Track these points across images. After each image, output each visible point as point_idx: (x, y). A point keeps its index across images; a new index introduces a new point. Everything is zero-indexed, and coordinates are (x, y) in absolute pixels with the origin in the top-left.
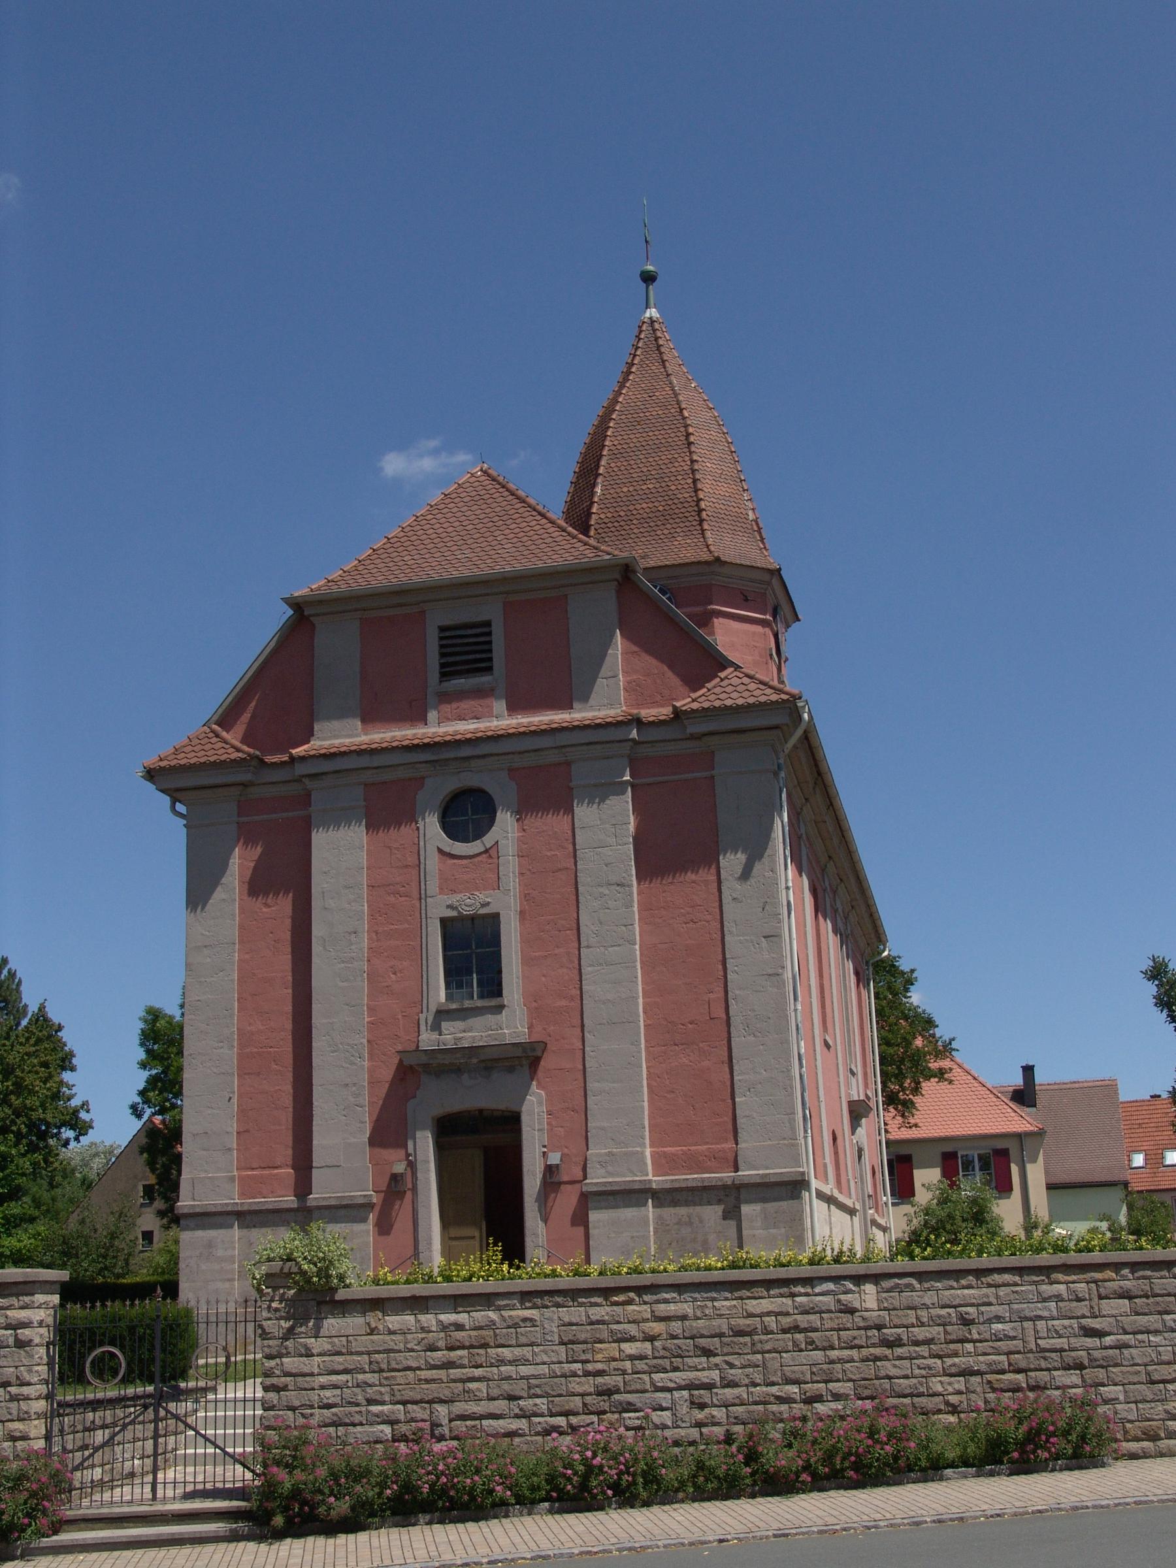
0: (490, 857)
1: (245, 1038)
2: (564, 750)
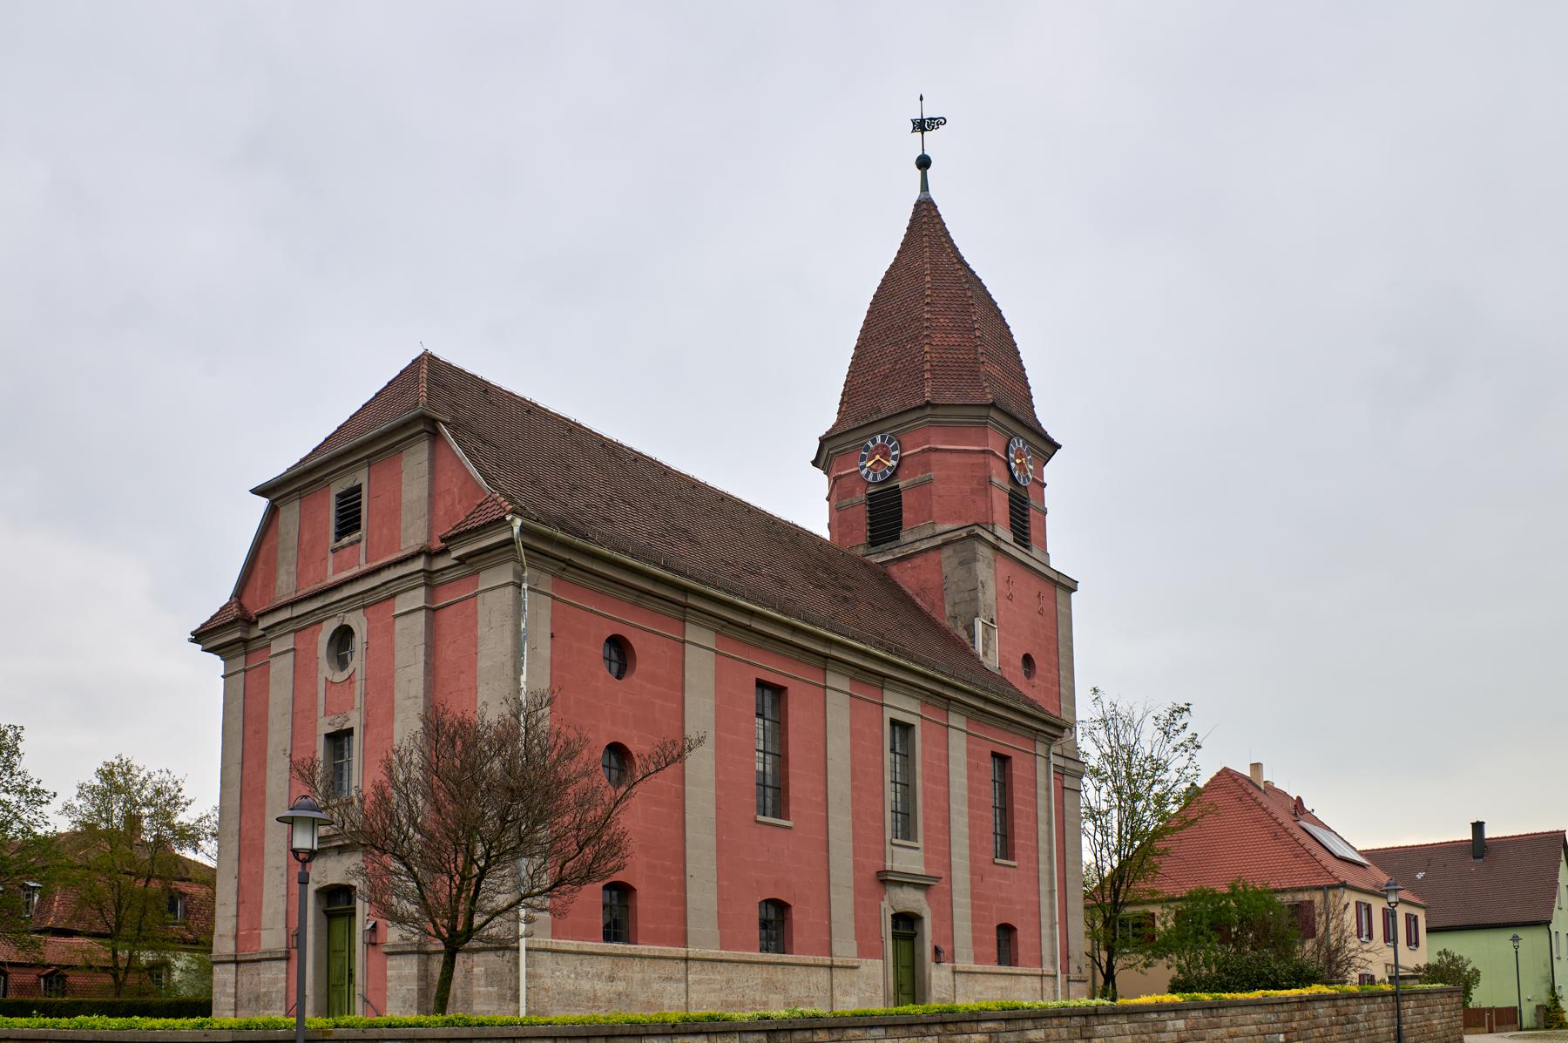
2: (388, 586)
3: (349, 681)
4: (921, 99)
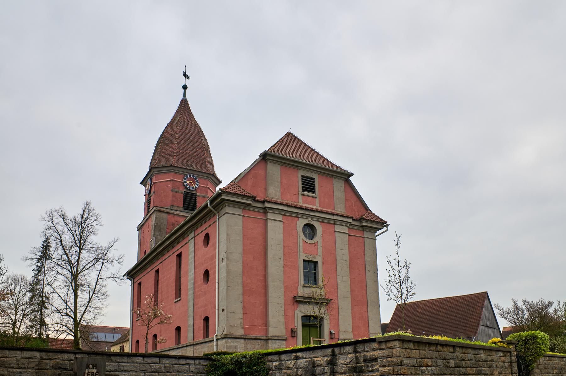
0: (315, 245)
1: (244, 285)
3: (314, 244)
4: (186, 67)
